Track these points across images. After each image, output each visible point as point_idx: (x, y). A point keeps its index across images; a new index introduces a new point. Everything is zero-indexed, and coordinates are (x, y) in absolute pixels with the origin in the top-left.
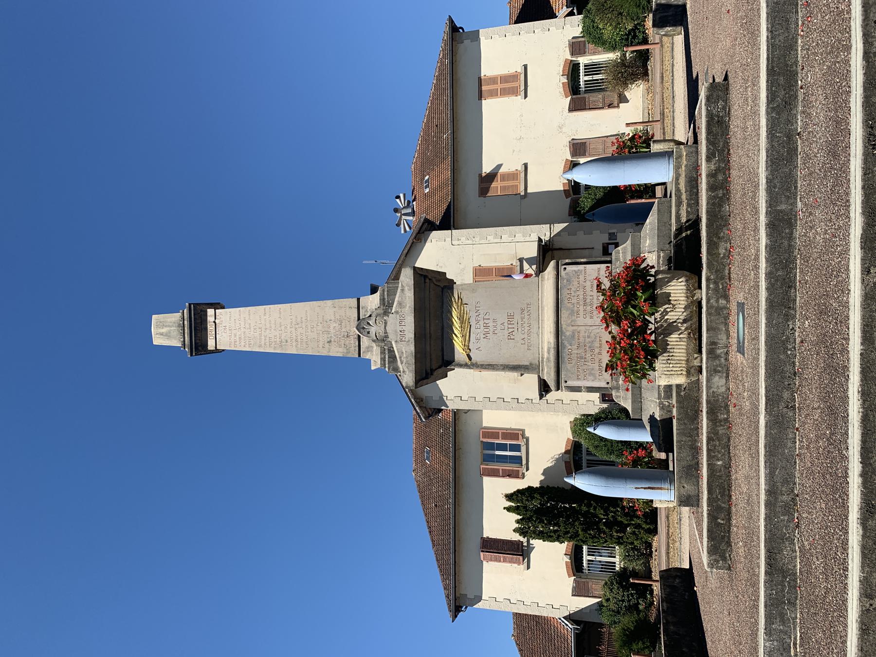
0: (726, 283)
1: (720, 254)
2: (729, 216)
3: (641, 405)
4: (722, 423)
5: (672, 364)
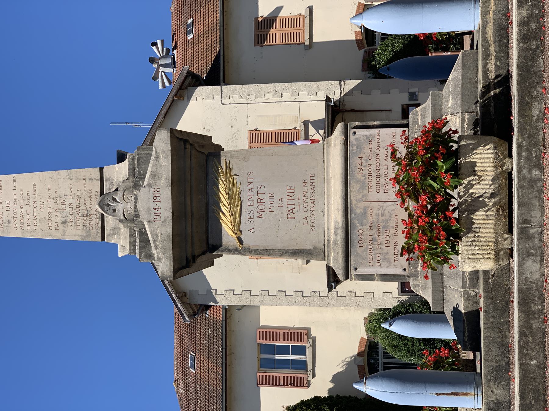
0: (540, 150)
1: (533, 116)
2: (544, 71)
3: (443, 296)
4: (536, 316)
5: (478, 246)
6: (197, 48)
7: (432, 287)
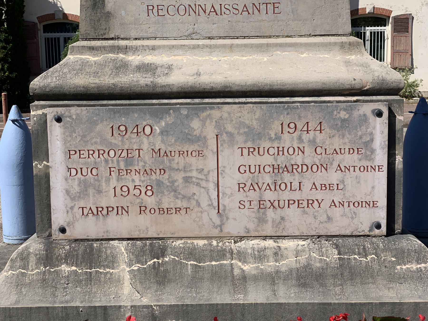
7: (17, 308)
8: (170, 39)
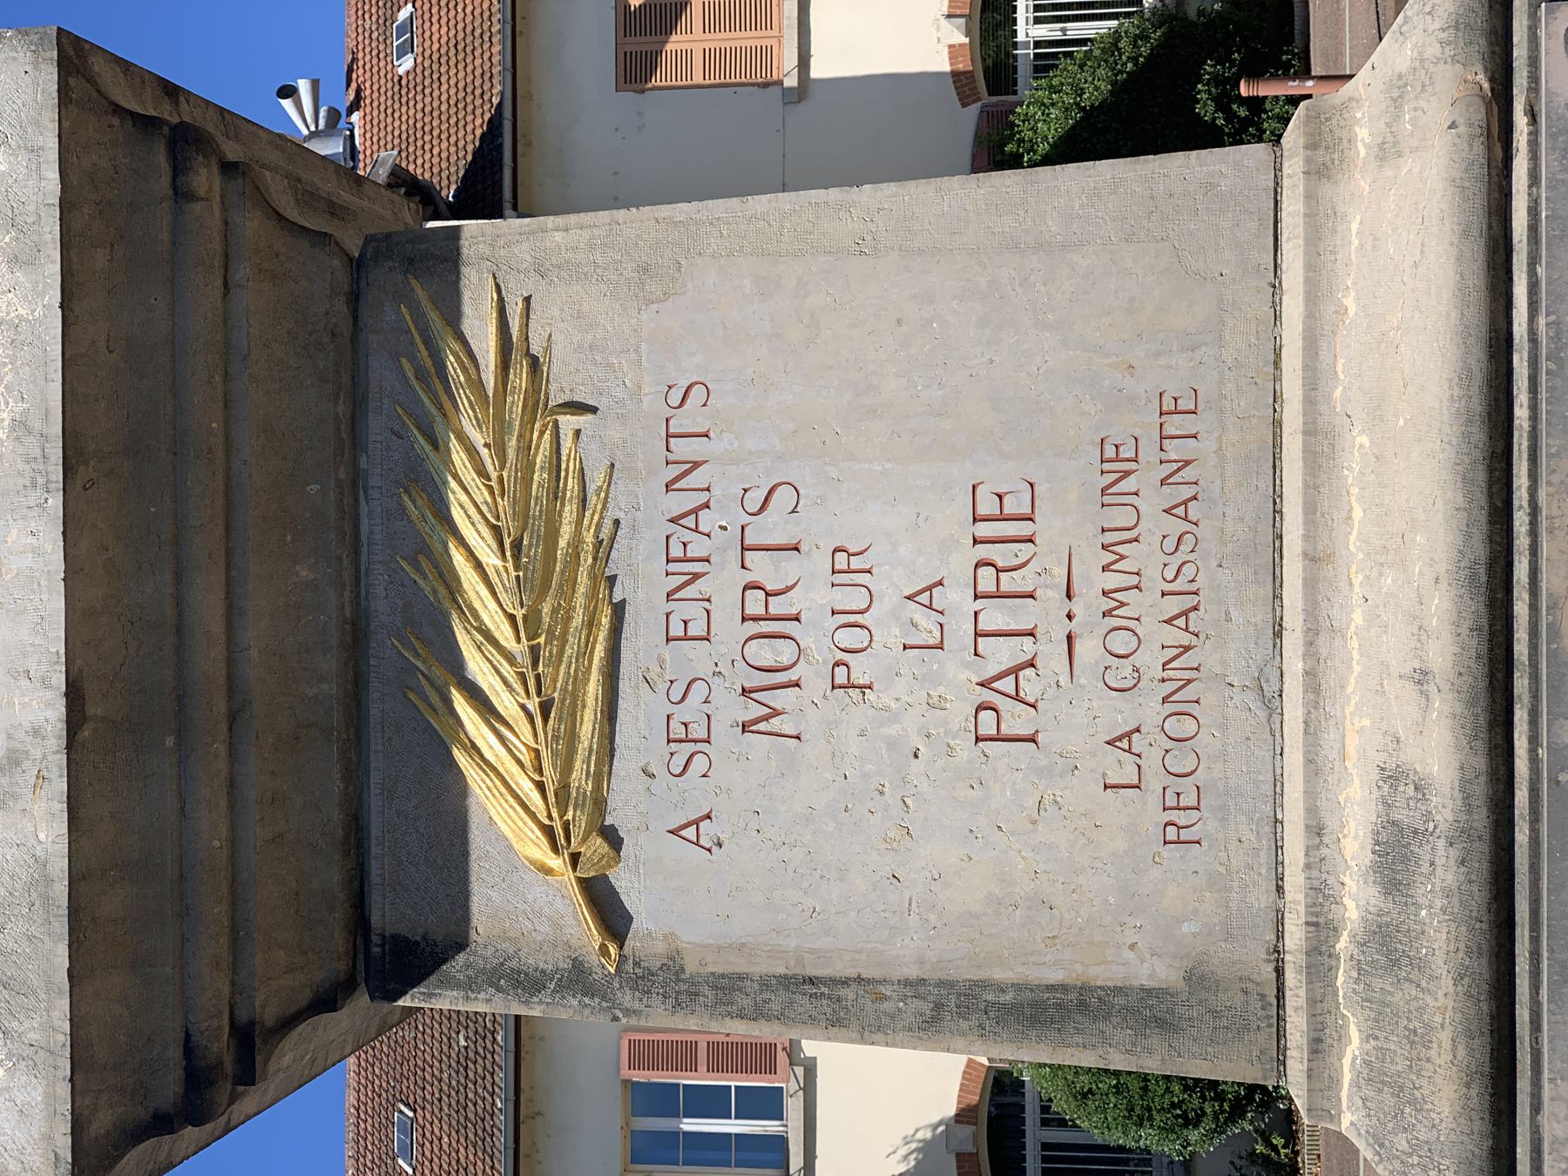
6: (427, 100)
8: (1278, 771)
